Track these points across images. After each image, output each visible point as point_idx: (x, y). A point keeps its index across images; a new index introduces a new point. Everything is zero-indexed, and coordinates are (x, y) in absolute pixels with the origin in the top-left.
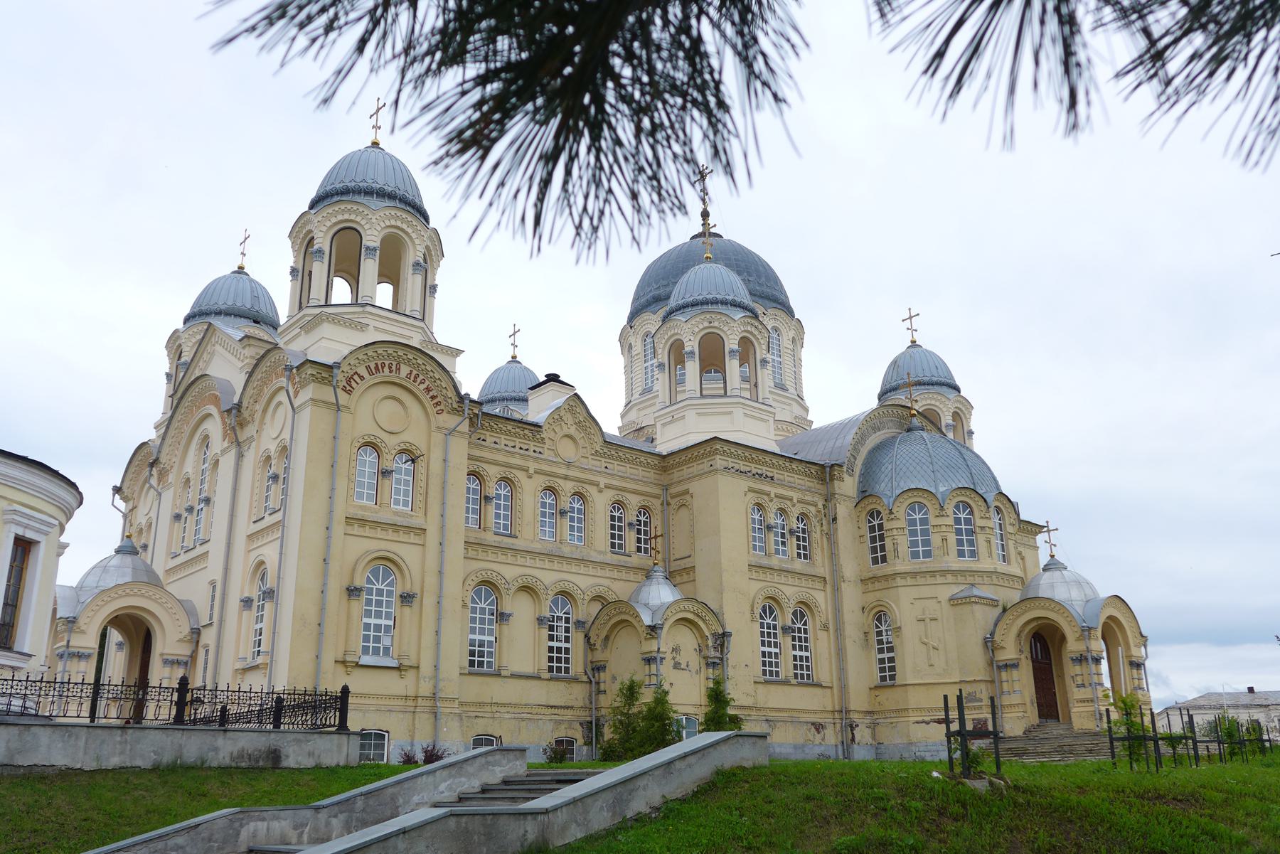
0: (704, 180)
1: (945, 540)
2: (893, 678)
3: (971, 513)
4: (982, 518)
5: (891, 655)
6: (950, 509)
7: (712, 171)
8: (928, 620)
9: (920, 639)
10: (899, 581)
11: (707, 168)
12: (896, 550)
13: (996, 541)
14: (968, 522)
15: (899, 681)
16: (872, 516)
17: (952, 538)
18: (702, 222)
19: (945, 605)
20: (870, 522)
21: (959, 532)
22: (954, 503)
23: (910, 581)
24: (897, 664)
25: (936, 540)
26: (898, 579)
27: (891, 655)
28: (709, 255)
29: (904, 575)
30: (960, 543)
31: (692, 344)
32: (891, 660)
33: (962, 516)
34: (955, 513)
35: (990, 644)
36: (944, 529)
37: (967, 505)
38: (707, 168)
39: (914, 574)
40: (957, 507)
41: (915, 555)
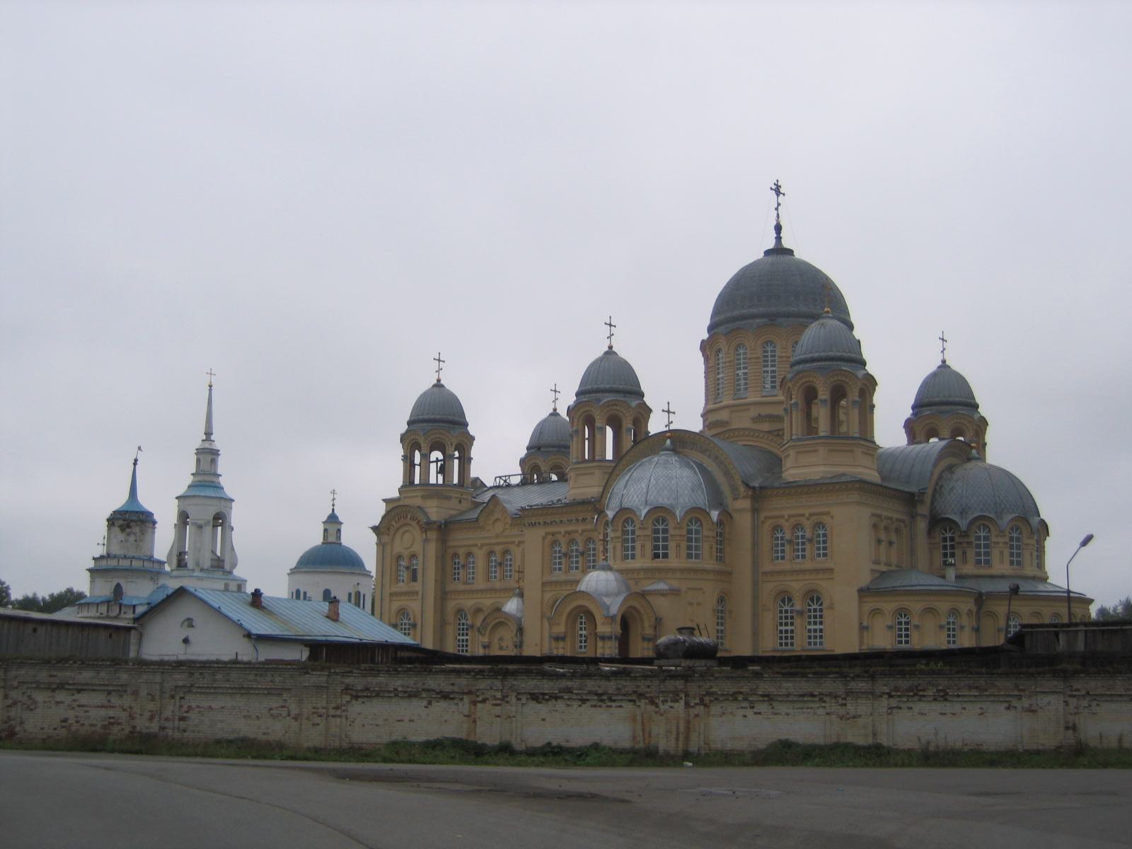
1: (1002, 553)
17: (1007, 552)
18: (775, 235)
21: (1012, 547)
28: (829, 309)
30: (1012, 555)
36: (1001, 545)
37: (1018, 528)
41: (979, 562)
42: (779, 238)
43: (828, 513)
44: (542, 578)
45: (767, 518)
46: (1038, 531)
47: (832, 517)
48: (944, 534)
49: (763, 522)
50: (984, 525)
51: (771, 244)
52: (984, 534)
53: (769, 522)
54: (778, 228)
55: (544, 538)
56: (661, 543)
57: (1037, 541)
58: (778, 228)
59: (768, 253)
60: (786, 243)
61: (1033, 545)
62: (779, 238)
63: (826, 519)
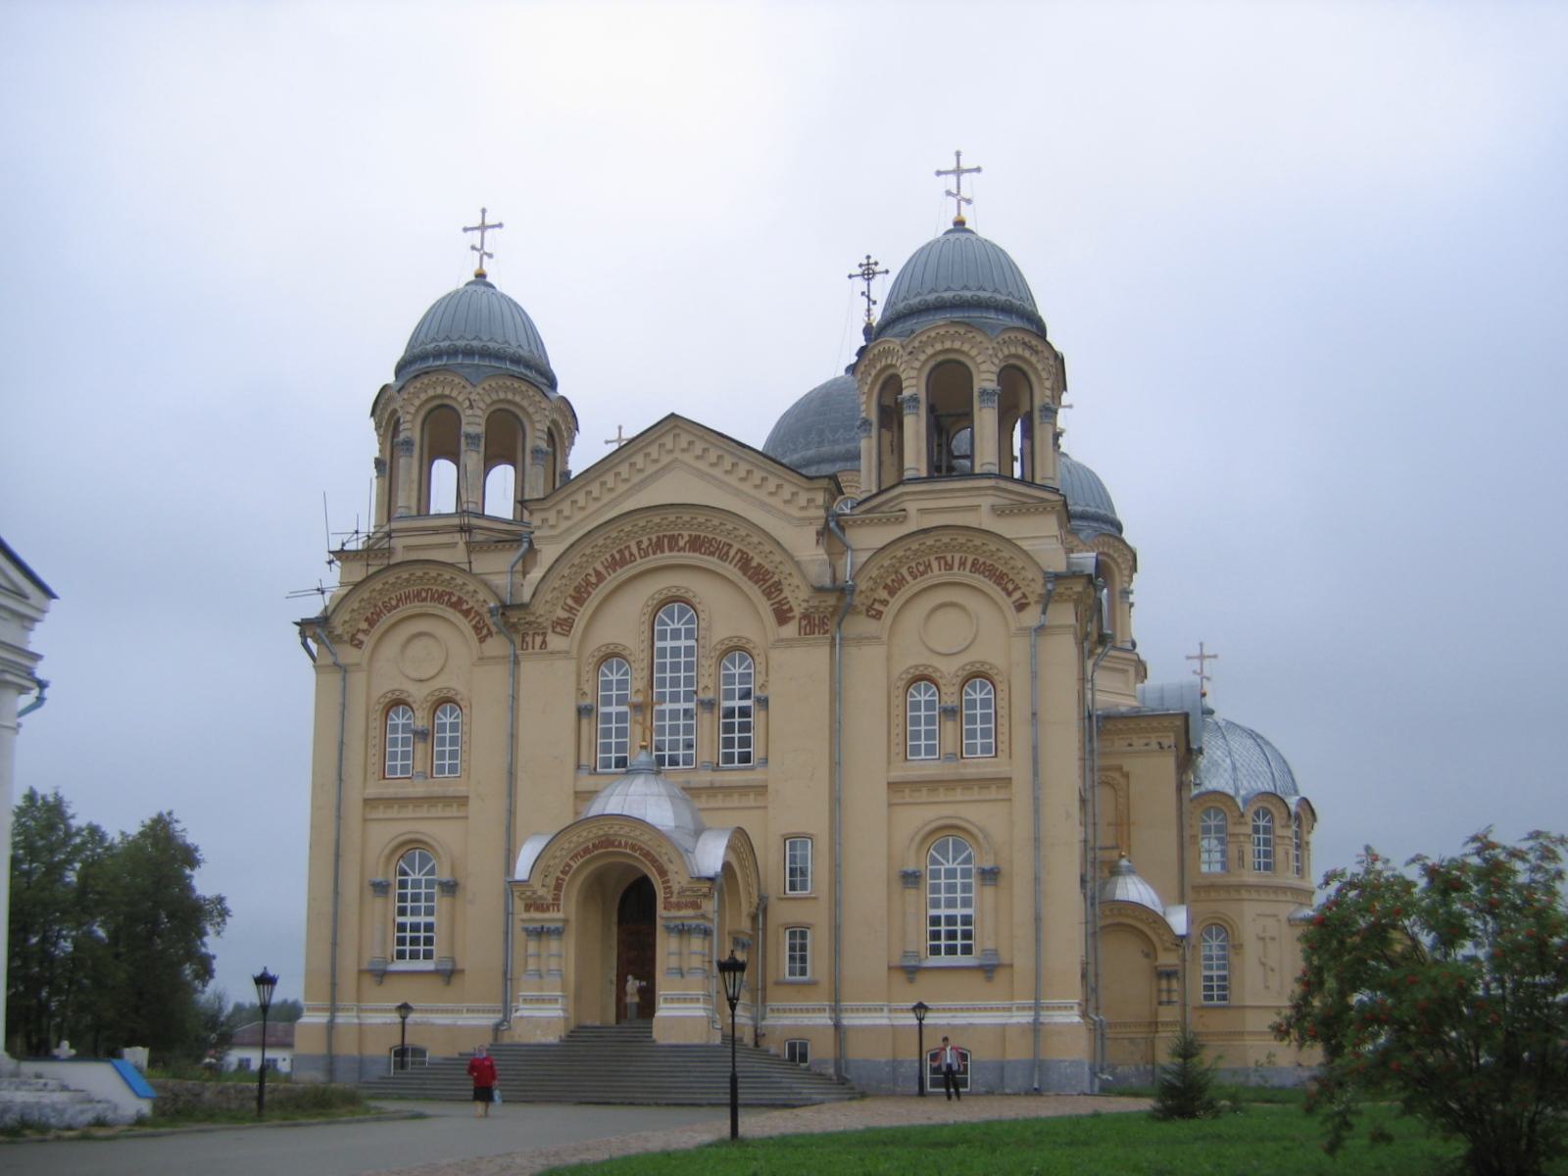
0: (869, 279)
3: (1272, 820)
4: (1283, 827)
6: (1249, 817)
9: (1260, 960)
10: (1244, 894)
11: (876, 264)
12: (1241, 858)
14: (1267, 830)
15: (1234, 1001)
20: (1204, 821)
22: (1254, 808)
23: (1254, 896)
25: (1280, 851)
26: (1243, 891)
29: (1249, 887)
32: (1223, 978)
34: (1254, 821)
38: (876, 264)
39: (1257, 888)
40: (1257, 814)
46: (1298, 817)
48: (1204, 821)
57: (1296, 832)
61: (1291, 839)
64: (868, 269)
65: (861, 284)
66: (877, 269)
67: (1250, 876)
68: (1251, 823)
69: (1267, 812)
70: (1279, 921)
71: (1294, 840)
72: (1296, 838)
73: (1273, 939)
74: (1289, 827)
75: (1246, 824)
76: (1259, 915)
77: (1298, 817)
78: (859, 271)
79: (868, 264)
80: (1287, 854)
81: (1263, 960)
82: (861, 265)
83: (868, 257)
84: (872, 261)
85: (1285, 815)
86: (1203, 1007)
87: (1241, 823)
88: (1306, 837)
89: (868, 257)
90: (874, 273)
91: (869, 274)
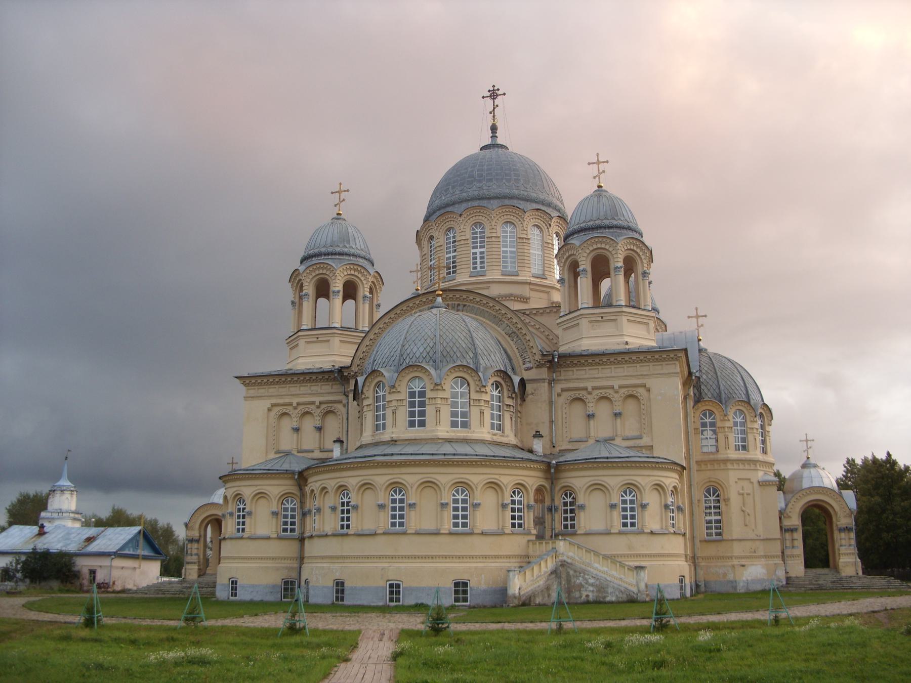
0: (494, 99)
2: (719, 534)
5: (708, 518)
7: (504, 94)
8: (745, 495)
10: (729, 466)
11: (498, 90)
13: (759, 438)
16: (705, 415)
19: (756, 485)
23: (736, 466)
24: (724, 524)
25: (750, 438)
27: (718, 518)
31: (618, 261)
33: (739, 420)
34: (734, 418)
35: (782, 514)
38: (498, 90)
40: (735, 414)
42: (494, 137)
43: (644, 386)
44: (266, 455)
45: (563, 390)
47: (649, 390)
49: (559, 395)
50: (739, 410)
51: (488, 141)
52: (710, 420)
53: (565, 395)
54: (494, 129)
55: (269, 410)
56: (417, 419)
58: (494, 129)
59: (483, 148)
60: (500, 141)
62: (494, 137)
63: (641, 391)
64: (494, 93)
65: (489, 101)
66: (499, 93)
67: (733, 454)
68: (732, 420)
69: (741, 411)
70: (752, 483)
71: (760, 430)
72: (762, 429)
73: (748, 494)
74: (756, 422)
75: (729, 420)
76: (738, 479)
77: (761, 415)
78: (488, 94)
79: (494, 90)
80: (755, 439)
81: (743, 508)
82: (489, 91)
83: (494, 86)
84: (496, 88)
85: (753, 414)
86: (706, 541)
87: (725, 420)
88: (767, 428)
89: (494, 86)
90: (497, 95)
91: (494, 96)
